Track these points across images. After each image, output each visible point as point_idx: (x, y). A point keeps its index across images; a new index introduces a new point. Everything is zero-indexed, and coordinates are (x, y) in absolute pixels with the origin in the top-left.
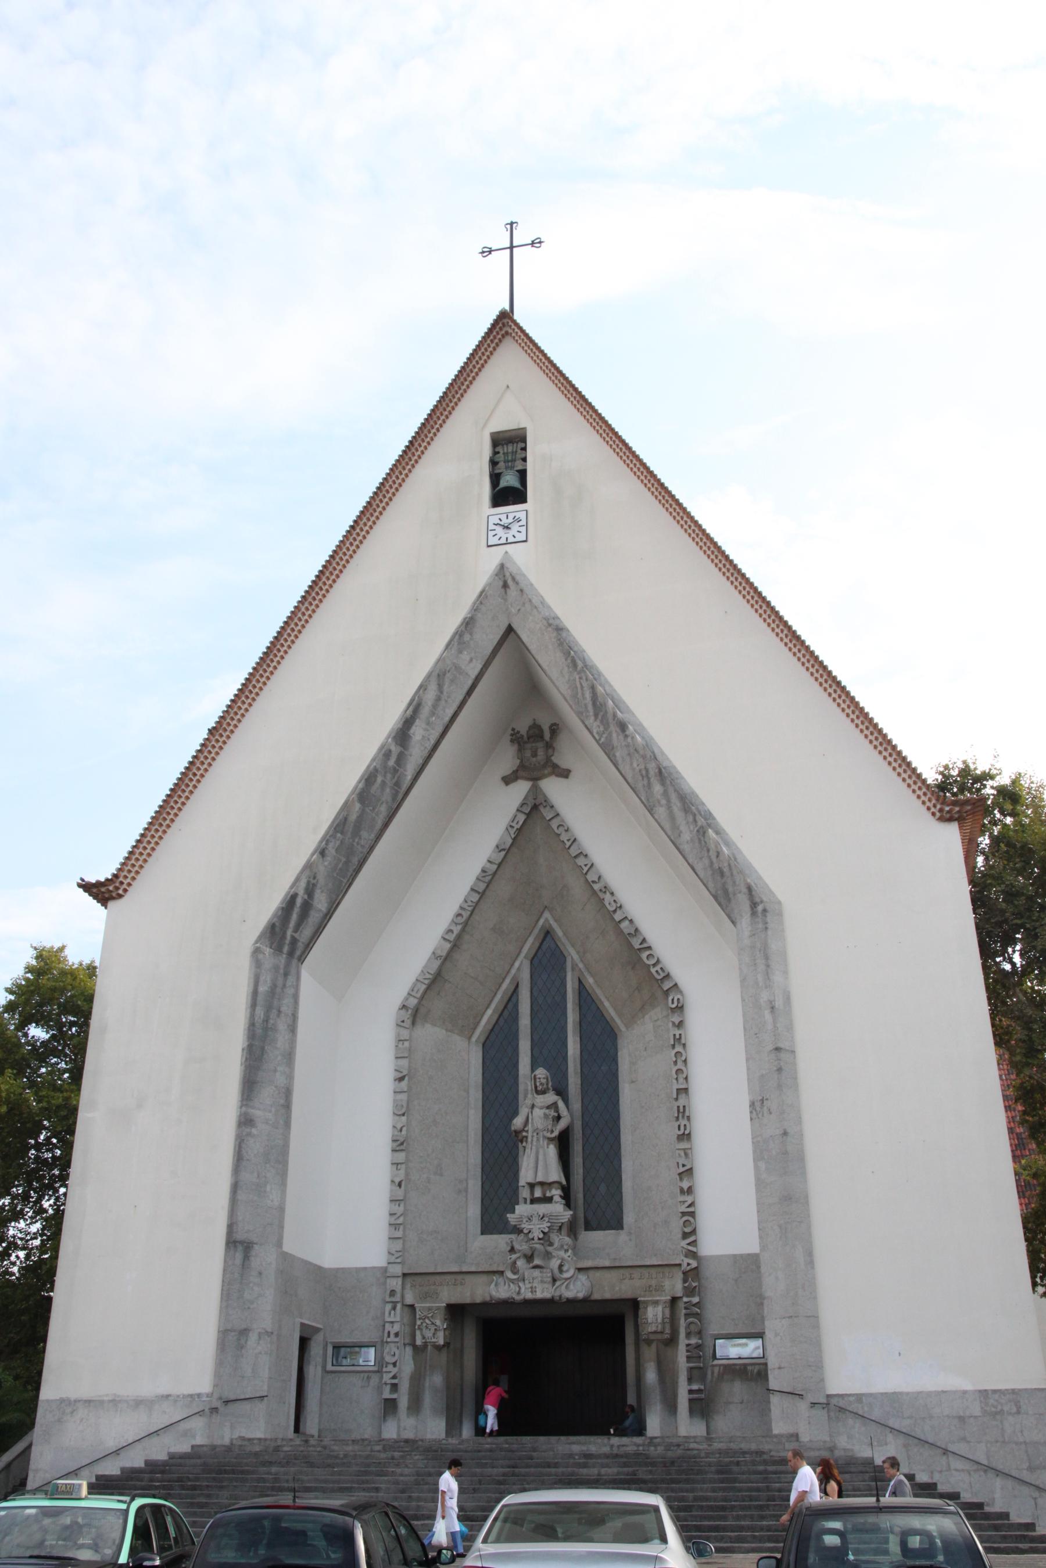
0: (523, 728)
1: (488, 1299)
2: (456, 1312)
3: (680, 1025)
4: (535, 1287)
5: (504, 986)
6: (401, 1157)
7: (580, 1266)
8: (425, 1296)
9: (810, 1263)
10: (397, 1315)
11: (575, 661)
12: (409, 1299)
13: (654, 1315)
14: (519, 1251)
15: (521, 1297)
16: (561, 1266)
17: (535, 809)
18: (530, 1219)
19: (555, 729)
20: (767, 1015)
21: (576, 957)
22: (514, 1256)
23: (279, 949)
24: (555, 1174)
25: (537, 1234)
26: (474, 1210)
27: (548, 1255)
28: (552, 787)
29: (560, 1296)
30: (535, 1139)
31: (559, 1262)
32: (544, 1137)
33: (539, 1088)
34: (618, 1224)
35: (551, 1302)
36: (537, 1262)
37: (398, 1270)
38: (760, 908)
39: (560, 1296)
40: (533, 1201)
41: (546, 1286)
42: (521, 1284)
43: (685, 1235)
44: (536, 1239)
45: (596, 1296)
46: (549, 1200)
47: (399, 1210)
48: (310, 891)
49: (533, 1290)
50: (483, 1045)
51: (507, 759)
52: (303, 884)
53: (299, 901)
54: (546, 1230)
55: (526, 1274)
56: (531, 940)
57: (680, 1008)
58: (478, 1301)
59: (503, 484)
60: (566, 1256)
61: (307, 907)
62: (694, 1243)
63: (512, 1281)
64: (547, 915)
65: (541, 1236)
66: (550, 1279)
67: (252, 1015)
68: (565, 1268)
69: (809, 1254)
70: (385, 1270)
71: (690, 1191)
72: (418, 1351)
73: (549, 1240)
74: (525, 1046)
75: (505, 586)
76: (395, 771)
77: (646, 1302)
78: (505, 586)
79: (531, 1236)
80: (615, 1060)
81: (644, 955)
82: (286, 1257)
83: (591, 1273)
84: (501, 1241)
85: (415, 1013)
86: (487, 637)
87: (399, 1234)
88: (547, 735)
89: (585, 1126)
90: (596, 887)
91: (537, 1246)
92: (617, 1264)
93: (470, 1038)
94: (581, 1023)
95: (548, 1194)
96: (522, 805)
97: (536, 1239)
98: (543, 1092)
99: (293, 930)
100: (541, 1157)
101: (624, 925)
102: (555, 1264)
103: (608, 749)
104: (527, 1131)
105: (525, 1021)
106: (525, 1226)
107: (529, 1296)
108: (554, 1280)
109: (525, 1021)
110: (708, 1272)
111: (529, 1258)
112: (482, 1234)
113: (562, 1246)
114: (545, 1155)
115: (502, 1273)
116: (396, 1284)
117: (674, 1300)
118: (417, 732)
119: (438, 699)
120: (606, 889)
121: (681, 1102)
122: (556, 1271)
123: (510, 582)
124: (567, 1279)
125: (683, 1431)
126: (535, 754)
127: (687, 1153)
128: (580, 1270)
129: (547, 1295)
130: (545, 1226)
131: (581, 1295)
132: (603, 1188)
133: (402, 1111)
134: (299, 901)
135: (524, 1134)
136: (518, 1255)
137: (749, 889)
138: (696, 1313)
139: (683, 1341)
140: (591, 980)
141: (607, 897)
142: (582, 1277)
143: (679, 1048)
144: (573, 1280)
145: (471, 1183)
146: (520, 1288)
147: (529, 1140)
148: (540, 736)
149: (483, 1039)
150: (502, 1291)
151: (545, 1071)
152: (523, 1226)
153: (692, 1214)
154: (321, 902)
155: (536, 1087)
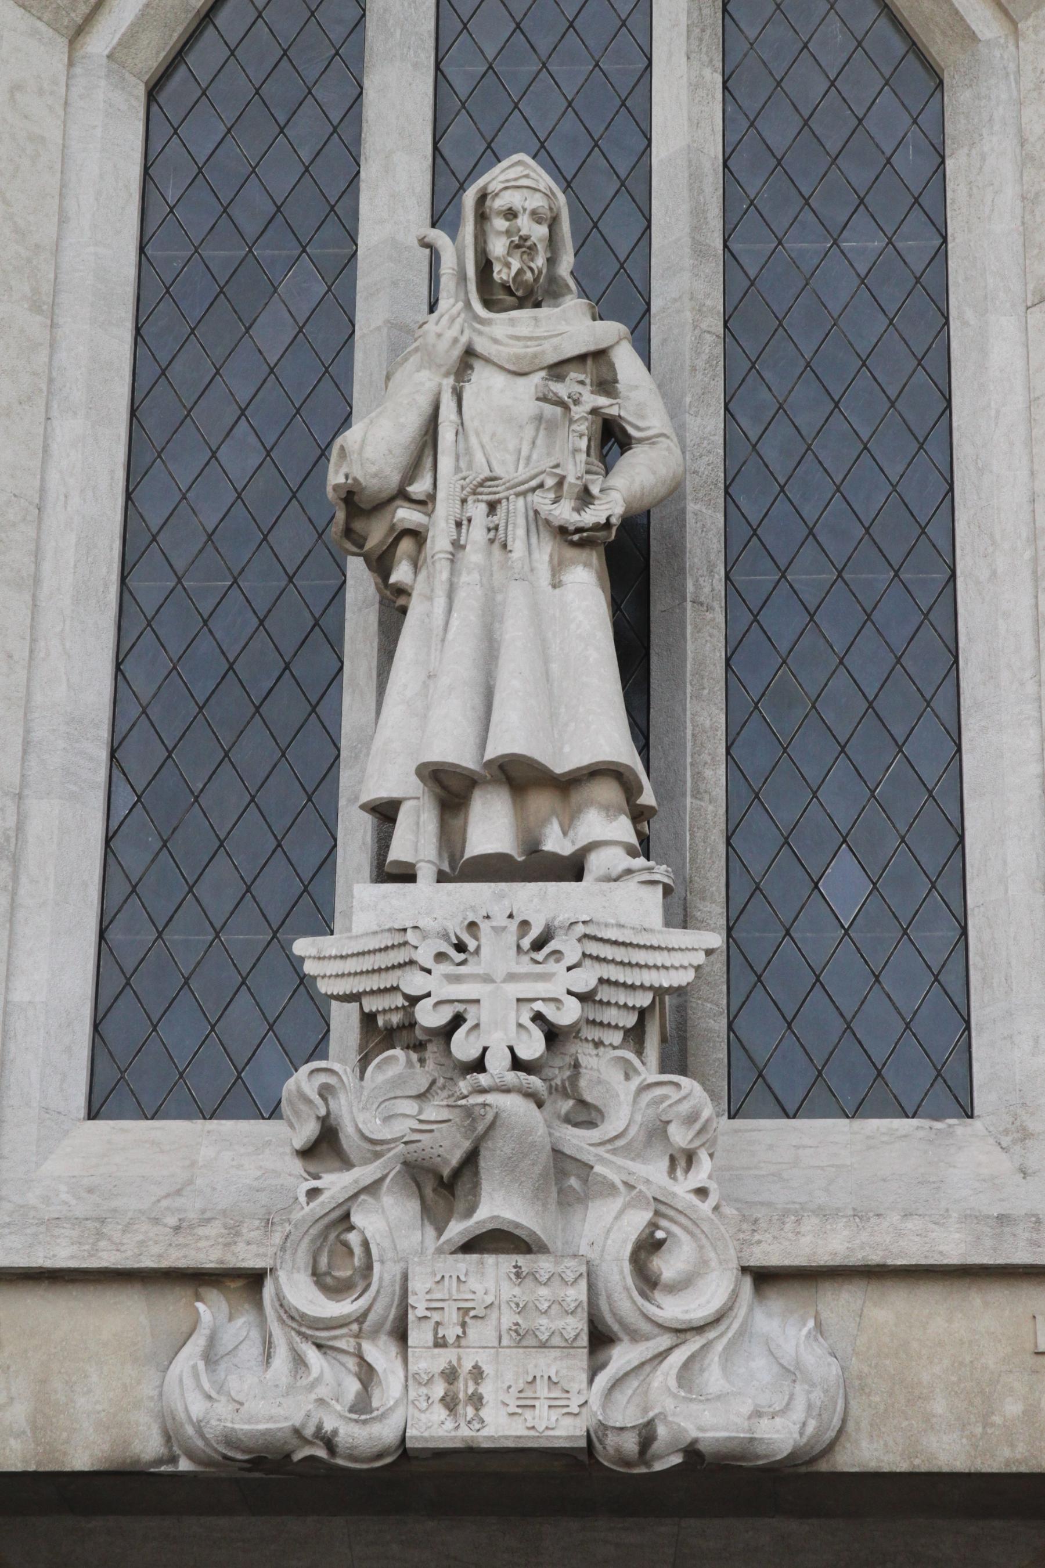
1: (148, 1446)
4: (491, 1373)
7: (772, 1254)
14: (376, 1147)
15: (384, 1433)
16: (648, 1246)
22: (336, 1183)
24: (601, 732)
25: (500, 1031)
26: (55, 975)
27: (566, 1179)
29: (647, 1436)
30: (477, 534)
31: (637, 1221)
32: (537, 520)
33: (500, 274)
34: (946, 1088)
36: (497, 1205)
39: (647, 1436)
40: (462, 869)
41: (547, 1364)
42: (380, 1354)
44: (498, 1064)
45: (869, 1452)
46: (572, 869)
49: (458, 1392)
50: (153, 93)
54: (568, 1014)
55: (419, 1285)
58: (81, 1461)
60: (681, 1189)
63: (316, 1332)
65: (533, 1046)
66: (577, 1326)
68: (668, 1266)
73: (569, 1089)
79: (463, 1046)
80: (929, 206)
83: (840, 1303)
89: (742, 539)
91: (512, 1105)
92: (1022, 1256)
93: (78, 32)
95: (556, 842)
97: (498, 1064)
98: (528, 296)
100: (515, 633)
102: (607, 1231)
104: (425, 504)
107: (434, 1427)
108: (600, 1338)
111: (442, 1186)
112: (93, 1113)
113: (658, 1131)
114: (536, 611)
115: (252, 1281)
122: (617, 1274)
124: (683, 1332)
128: (764, 1278)
129: (557, 1426)
130: (558, 989)
131: (781, 1434)
132: (845, 884)
135: (406, 515)
136: (363, 1174)
142: (783, 1328)
144: (721, 1339)
145: (44, 815)
146: (367, 1374)
147: (439, 540)
149: (151, 55)
150: (248, 1389)
151: (544, 180)
152: (413, 983)
155: (485, 267)
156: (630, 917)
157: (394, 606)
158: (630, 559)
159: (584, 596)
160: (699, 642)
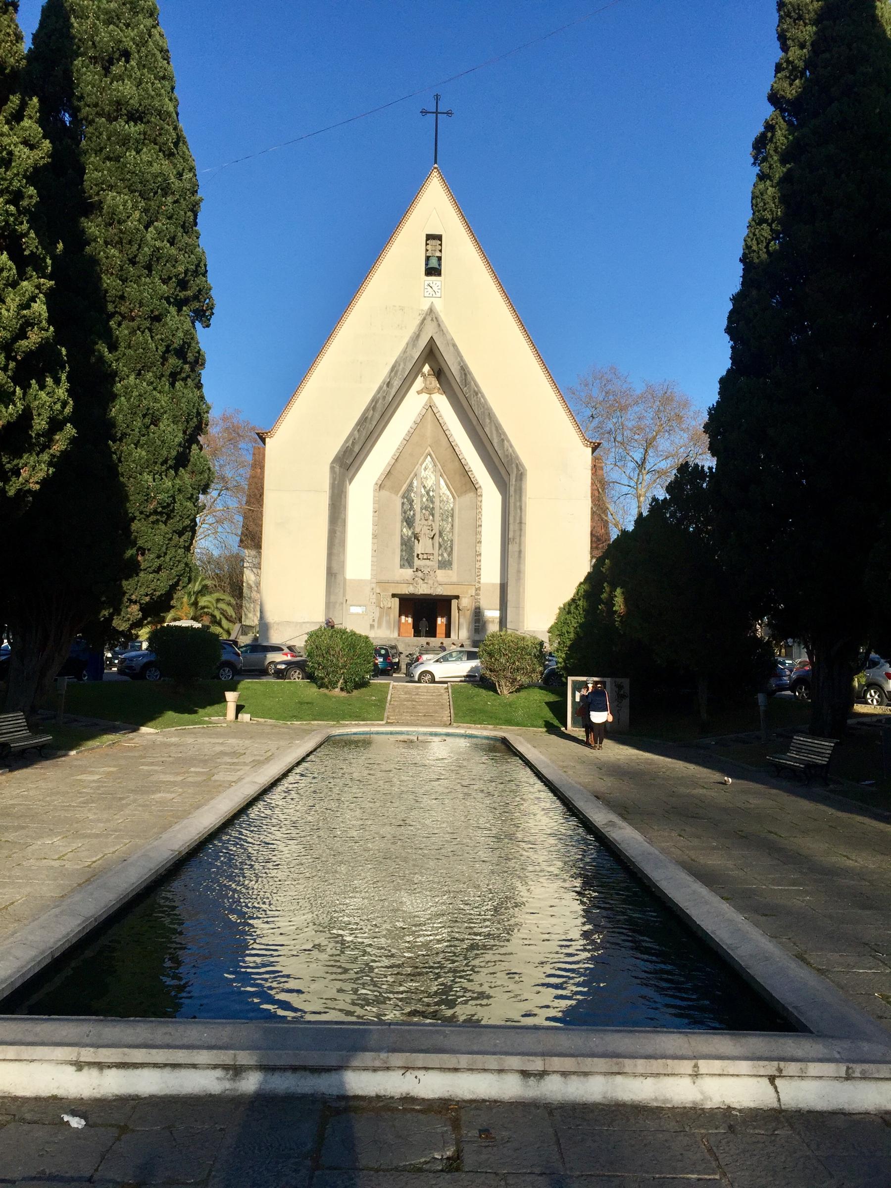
6: (376, 541)
37: (375, 581)
52: (351, 442)
57: (481, 496)
59: (430, 266)
85: (381, 487)
116: (374, 585)
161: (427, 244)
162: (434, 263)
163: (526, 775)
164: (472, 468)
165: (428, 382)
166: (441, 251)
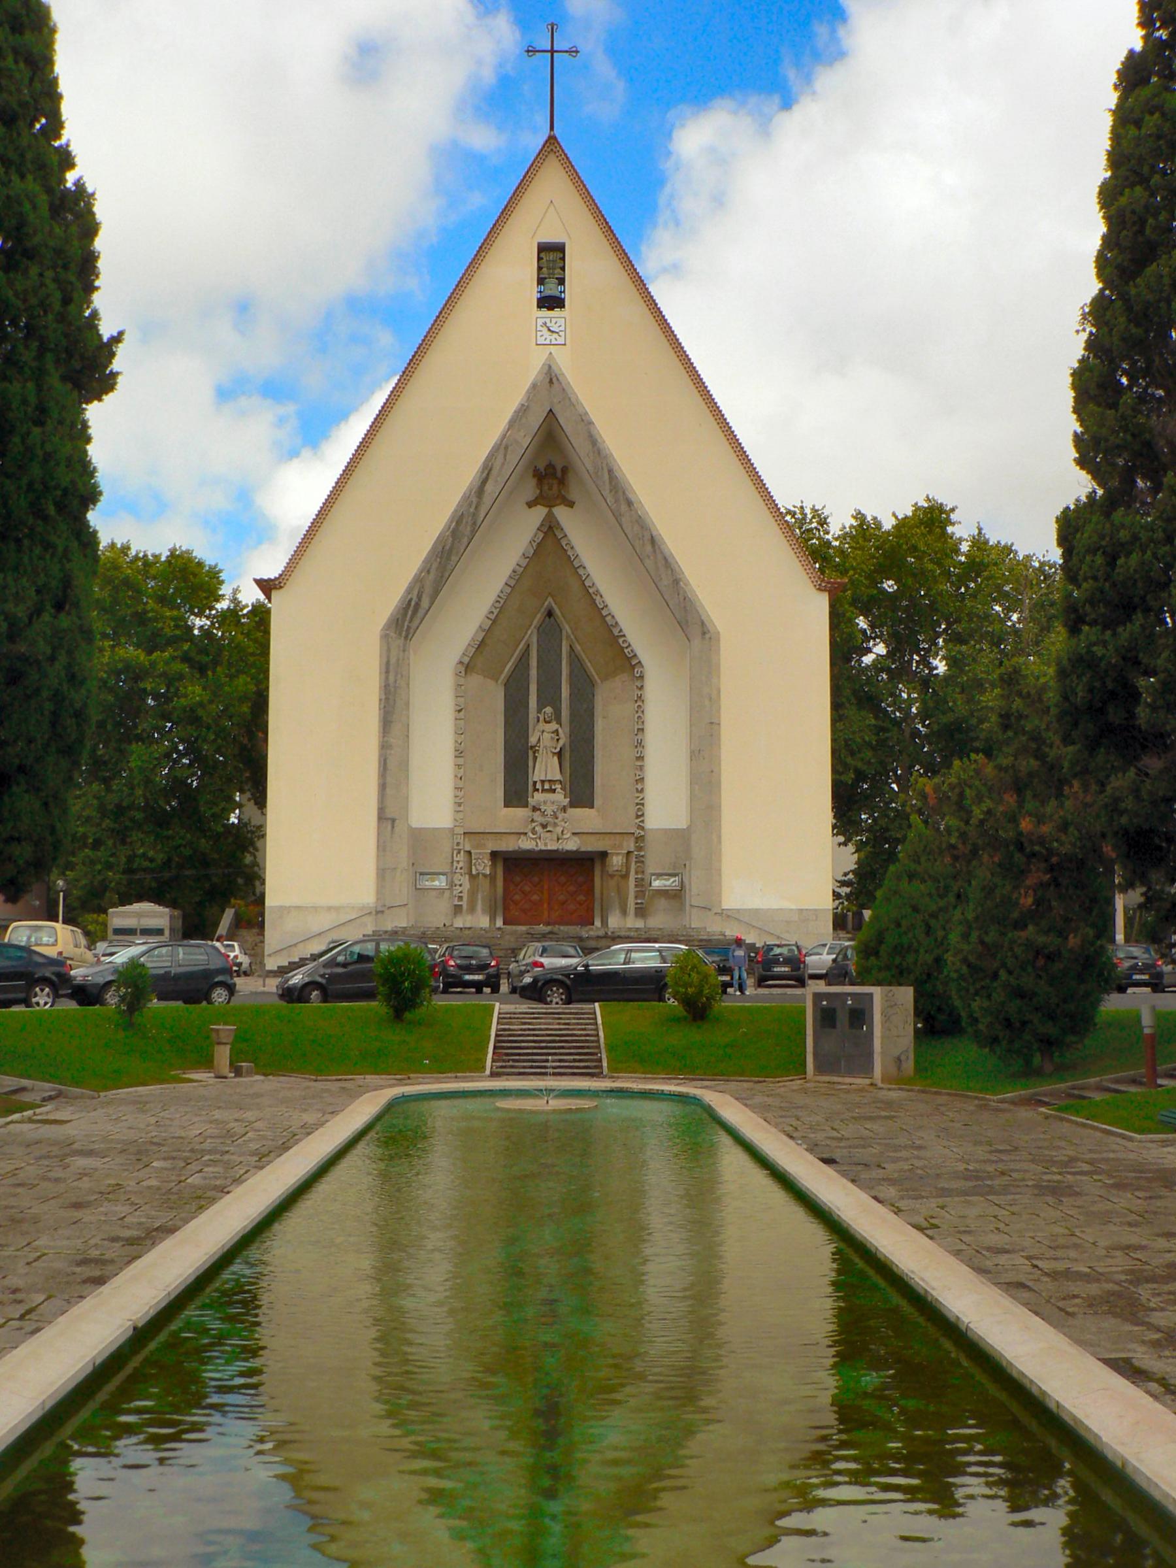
0: (541, 466)
2: (494, 855)
3: (641, 688)
5: (521, 646)
6: (461, 761)
8: (477, 847)
9: (720, 842)
10: (462, 857)
11: (593, 441)
12: (467, 849)
13: (616, 861)
17: (550, 528)
18: (545, 803)
19: (565, 470)
20: (707, 702)
21: (569, 631)
23: (400, 634)
24: (558, 777)
25: (549, 812)
27: (555, 825)
28: (561, 513)
35: (557, 851)
38: (707, 636)
40: (543, 790)
43: (638, 817)
45: (583, 849)
46: (554, 791)
47: (460, 794)
48: (419, 597)
51: (530, 489)
52: (416, 592)
53: (413, 603)
56: (539, 616)
57: (642, 677)
61: (417, 605)
62: (642, 821)
64: (550, 599)
67: (387, 678)
69: (719, 837)
70: (452, 830)
71: (642, 791)
72: (473, 877)
74: (533, 688)
75: (551, 382)
76: (474, 514)
77: (613, 854)
78: (551, 382)
81: (620, 641)
82: (410, 828)
84: (520, 813)
85: (467, 667)
86: (536, 419)
87: (461, 808)
88: (559, 474)
90: (591, 591)
94: (571, 674)
96: (542, 525)
99: (408, 620)
101: (608, 619)
103: (617, 517)
105: (533, 672)
106: (543, 808)
107: (543, 848)
109: (533, 672)
110: (649, 838)
111: (544, 826)
117: (629, 853)
118: (489, 487)
119: (503, 464)
120: (598, 592)
121: (639, 737)
123: (554, 380)
125: (629, 925)
126: (550, 489)
127: (641, 768)
130: (555, 808)
133: (459, 732)
134: (413, 603)
137: (703, 623)
138: (641, 861)
139: (632, 876)
140: (579, 648)
141: (598, 599)
142: (576, 838)
143: (639, 703)
148: (554, 475)
150: (526, 844)
153: (643, 804)
154: (425, 603)
156: (560, 798)
157: (535, 758)
158: (560, 755)
159: (556, 758)
160: (567, 764)
161: (539, 259)
162: (551, 289)
163: (725, 1140)
164: (626, 631)
165: (546, 488)
166: (563, 269)
